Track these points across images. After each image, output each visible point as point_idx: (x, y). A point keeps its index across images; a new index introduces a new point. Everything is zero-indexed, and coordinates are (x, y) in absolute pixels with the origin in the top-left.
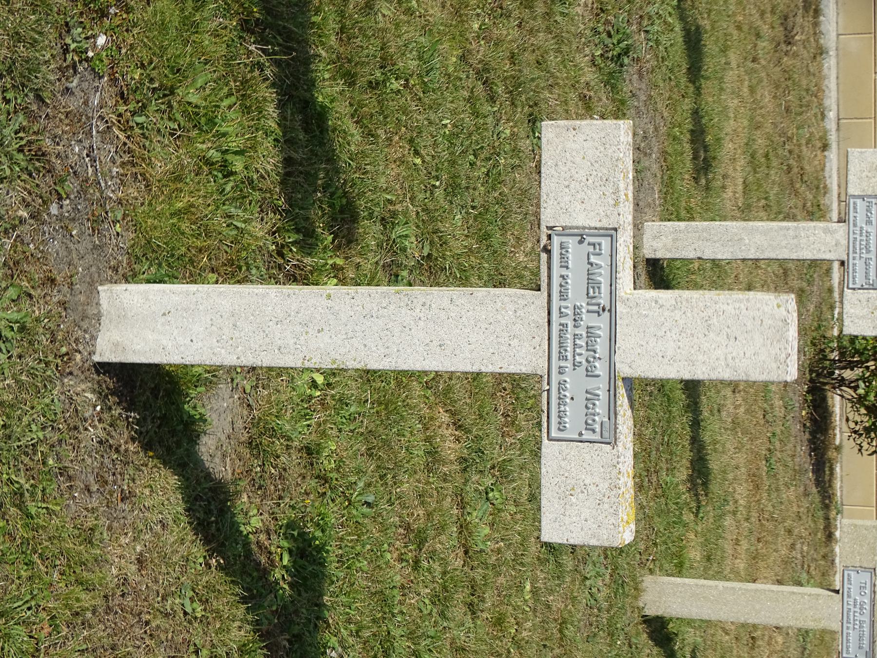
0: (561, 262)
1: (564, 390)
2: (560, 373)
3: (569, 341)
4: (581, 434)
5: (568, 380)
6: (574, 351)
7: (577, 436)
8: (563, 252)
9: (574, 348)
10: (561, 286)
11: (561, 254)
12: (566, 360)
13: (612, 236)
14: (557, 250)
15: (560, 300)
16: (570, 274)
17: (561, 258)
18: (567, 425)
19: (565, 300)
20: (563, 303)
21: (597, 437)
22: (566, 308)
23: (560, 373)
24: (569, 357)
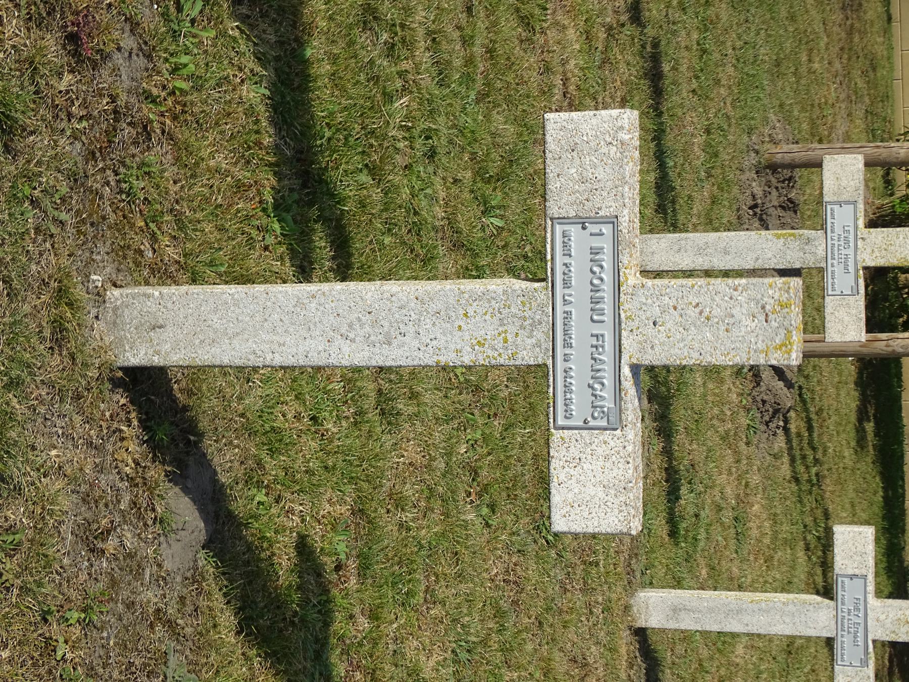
0: (564, 250)
2: (565, 360)
3: (573, 328)
4: (585, 422)
5: (573, 367)
7: (581, 424)
8: (566, 241)
10: (564, 274)
11: (564, 242)
12: (571, 347)
14: (560, 269)
15: (564, 288)
17: (564, 246)
18: (574, 413)
19: (569, 287)
20: (567, 291)
21: (604, 423)
22: (570, 295)
23: (565, 360)
24: (574, 345)
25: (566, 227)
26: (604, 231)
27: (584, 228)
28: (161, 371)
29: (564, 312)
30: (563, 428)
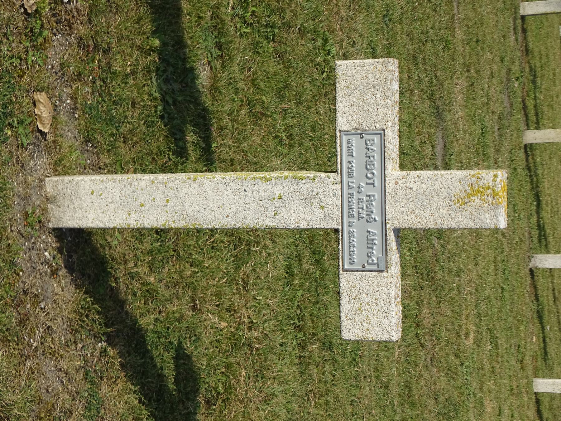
2: (349, 226)
4: (364, 266)
5: (355, 230)
10: (349, 168)
11: (348, 147)
12: (354, 217)
13: (381, 134)
18: (355, 260)
19: (352, 177)
20: (350, 180)
21: (375, 267)
23: (349, 226)
24: (355, 216)
25: (349, 137)
27: (362, 138)
30: (347, 271)
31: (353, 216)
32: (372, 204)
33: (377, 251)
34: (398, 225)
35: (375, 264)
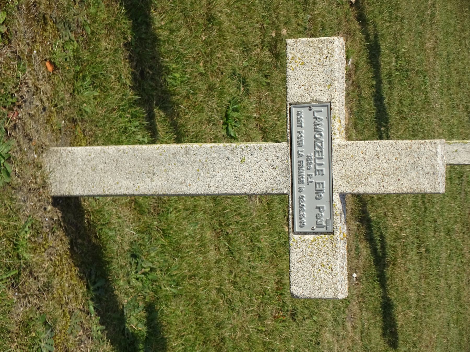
0: (298, 124)
1: (302, 202)
2: (299, 191)
4: (313, 229)
5: (304, 196)
6: (308, 180)
7: (310, 230)
9: (308, 178)
10: (298, 138)
11: (298, 119)
12: (303, 183)
15: (298, 147)
16: (303, 131)
18: (305, 224)
19: (301, 146)
20: (300, 149)
21: (324, 230)
24: (304, 182)
25: (299, 109)
26: (323, 110)
28: (77, 198)
29: (299, 162)
30: (298, 233)
31: (302, 182)
32: (321, 196)
33: (325, 215)
34: (343, 190)
35: (323, 227)
